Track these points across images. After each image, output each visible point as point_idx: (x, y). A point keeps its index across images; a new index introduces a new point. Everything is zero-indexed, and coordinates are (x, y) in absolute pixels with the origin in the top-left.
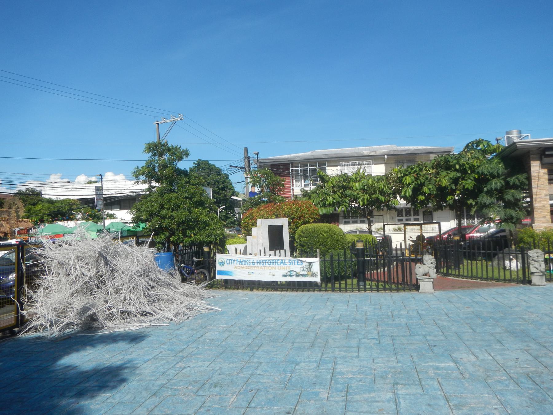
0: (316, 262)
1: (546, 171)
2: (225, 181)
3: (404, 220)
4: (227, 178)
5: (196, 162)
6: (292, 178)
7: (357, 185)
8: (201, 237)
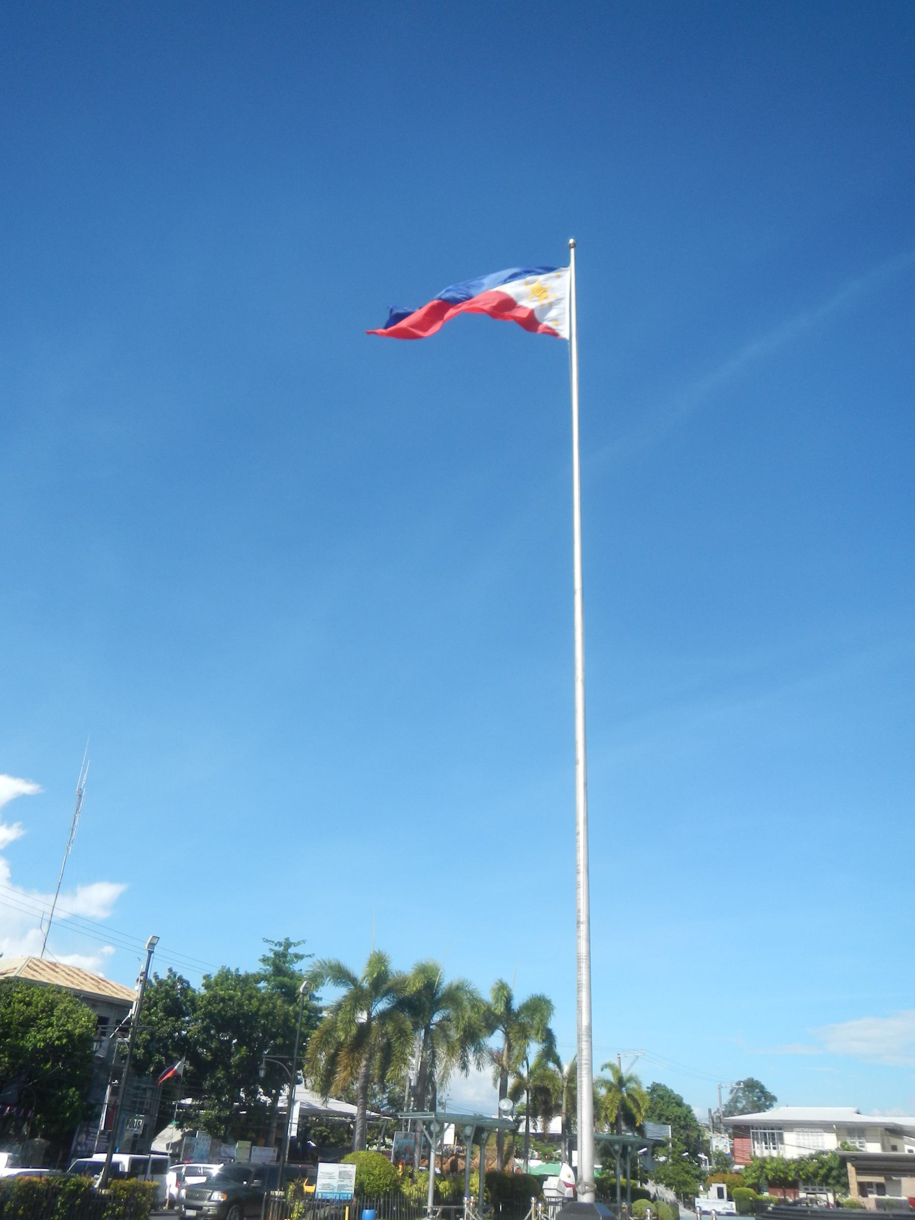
0: (734, 1204)
2: (687, 1116)
3: (810, 1189)
4: (690, 1111)
5: (650, 1086)
6: (753, 1138)
7: (768, 1166)
8: (688, 1190)
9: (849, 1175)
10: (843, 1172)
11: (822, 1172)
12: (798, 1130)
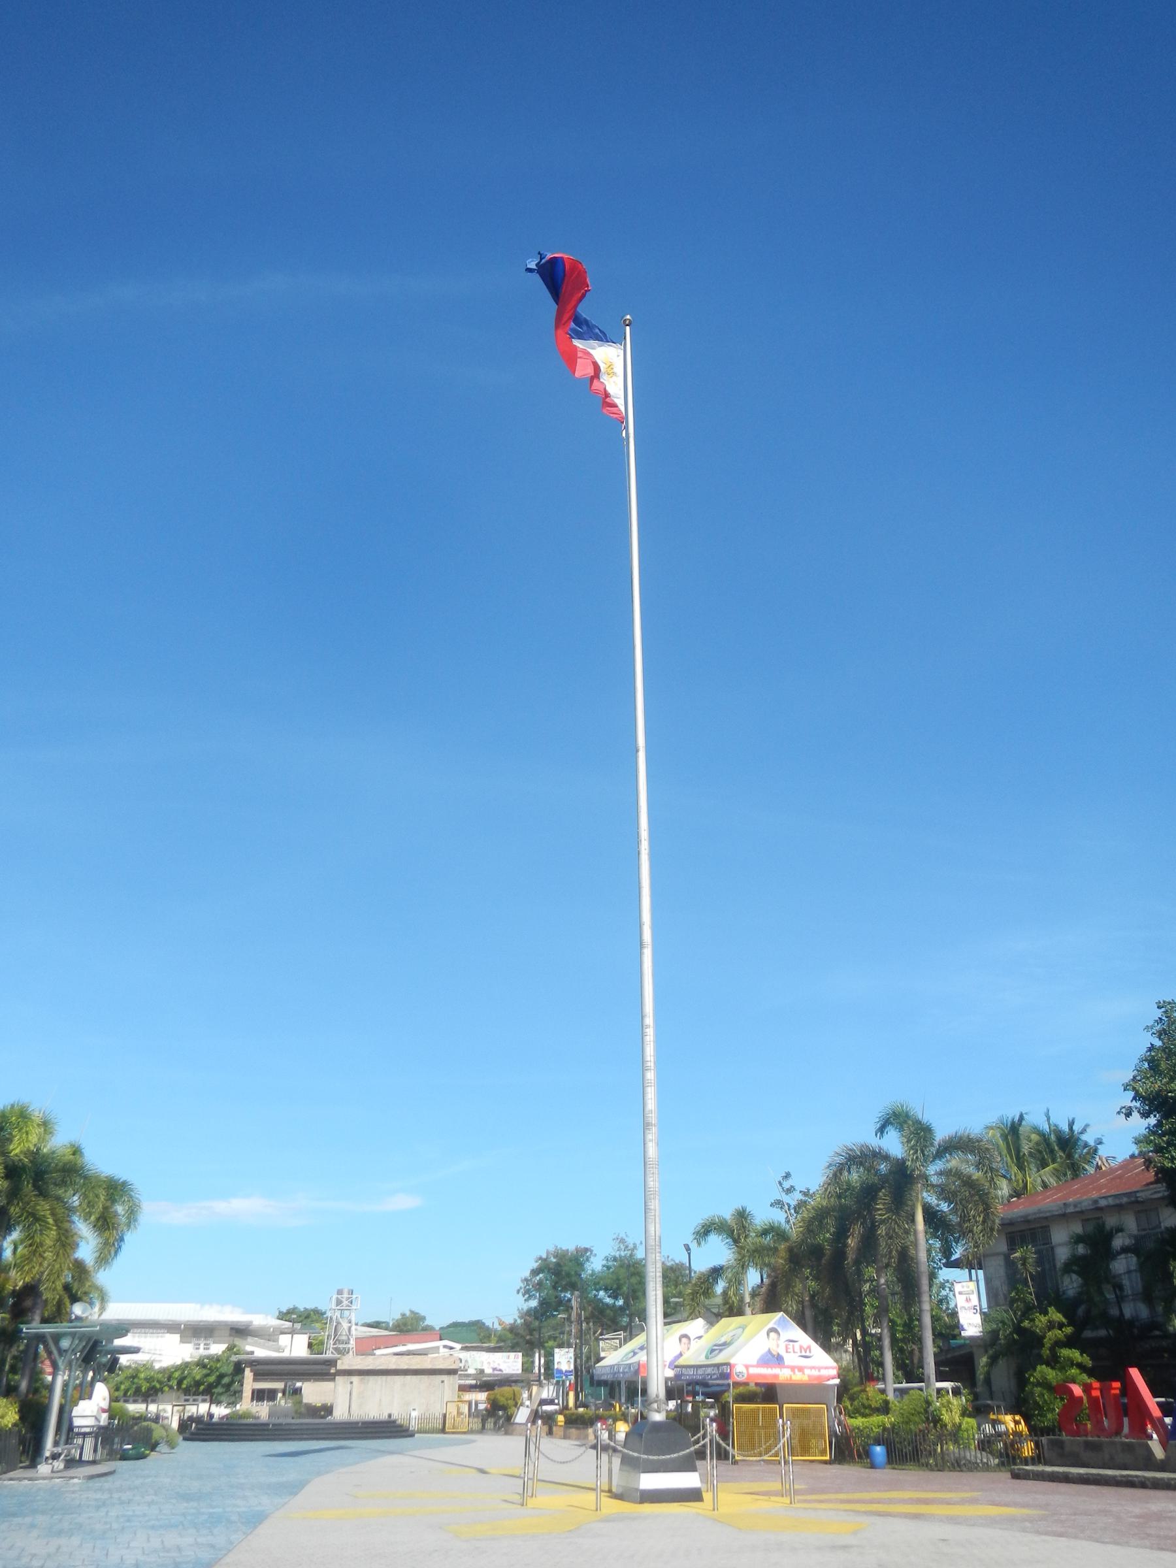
1: (252, 1374)
7: (142, 1376)
9: (245, 1381)
10: (237, 1378)
11: (212, 1379)
12: (135, 1330)
